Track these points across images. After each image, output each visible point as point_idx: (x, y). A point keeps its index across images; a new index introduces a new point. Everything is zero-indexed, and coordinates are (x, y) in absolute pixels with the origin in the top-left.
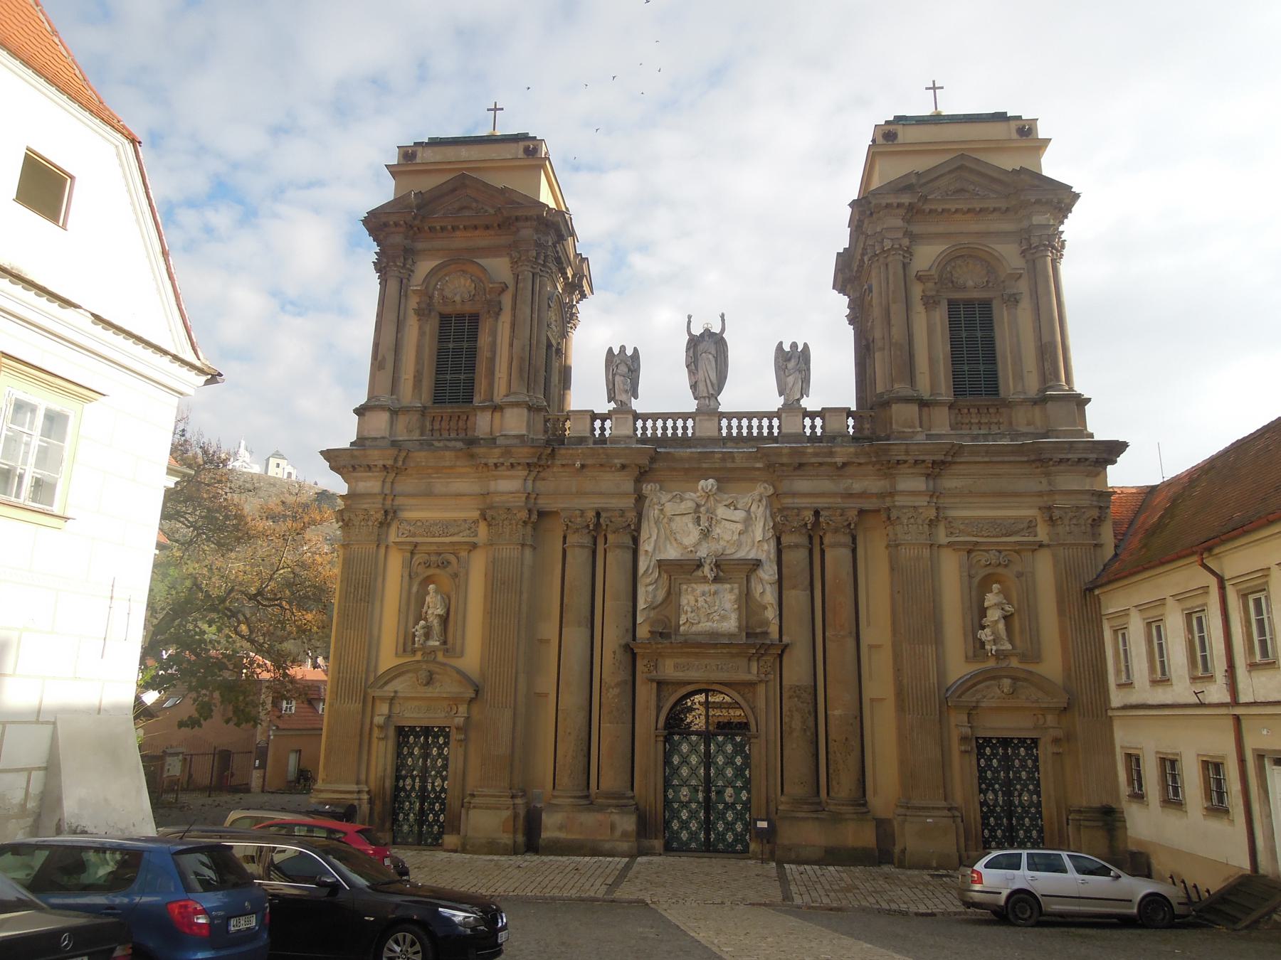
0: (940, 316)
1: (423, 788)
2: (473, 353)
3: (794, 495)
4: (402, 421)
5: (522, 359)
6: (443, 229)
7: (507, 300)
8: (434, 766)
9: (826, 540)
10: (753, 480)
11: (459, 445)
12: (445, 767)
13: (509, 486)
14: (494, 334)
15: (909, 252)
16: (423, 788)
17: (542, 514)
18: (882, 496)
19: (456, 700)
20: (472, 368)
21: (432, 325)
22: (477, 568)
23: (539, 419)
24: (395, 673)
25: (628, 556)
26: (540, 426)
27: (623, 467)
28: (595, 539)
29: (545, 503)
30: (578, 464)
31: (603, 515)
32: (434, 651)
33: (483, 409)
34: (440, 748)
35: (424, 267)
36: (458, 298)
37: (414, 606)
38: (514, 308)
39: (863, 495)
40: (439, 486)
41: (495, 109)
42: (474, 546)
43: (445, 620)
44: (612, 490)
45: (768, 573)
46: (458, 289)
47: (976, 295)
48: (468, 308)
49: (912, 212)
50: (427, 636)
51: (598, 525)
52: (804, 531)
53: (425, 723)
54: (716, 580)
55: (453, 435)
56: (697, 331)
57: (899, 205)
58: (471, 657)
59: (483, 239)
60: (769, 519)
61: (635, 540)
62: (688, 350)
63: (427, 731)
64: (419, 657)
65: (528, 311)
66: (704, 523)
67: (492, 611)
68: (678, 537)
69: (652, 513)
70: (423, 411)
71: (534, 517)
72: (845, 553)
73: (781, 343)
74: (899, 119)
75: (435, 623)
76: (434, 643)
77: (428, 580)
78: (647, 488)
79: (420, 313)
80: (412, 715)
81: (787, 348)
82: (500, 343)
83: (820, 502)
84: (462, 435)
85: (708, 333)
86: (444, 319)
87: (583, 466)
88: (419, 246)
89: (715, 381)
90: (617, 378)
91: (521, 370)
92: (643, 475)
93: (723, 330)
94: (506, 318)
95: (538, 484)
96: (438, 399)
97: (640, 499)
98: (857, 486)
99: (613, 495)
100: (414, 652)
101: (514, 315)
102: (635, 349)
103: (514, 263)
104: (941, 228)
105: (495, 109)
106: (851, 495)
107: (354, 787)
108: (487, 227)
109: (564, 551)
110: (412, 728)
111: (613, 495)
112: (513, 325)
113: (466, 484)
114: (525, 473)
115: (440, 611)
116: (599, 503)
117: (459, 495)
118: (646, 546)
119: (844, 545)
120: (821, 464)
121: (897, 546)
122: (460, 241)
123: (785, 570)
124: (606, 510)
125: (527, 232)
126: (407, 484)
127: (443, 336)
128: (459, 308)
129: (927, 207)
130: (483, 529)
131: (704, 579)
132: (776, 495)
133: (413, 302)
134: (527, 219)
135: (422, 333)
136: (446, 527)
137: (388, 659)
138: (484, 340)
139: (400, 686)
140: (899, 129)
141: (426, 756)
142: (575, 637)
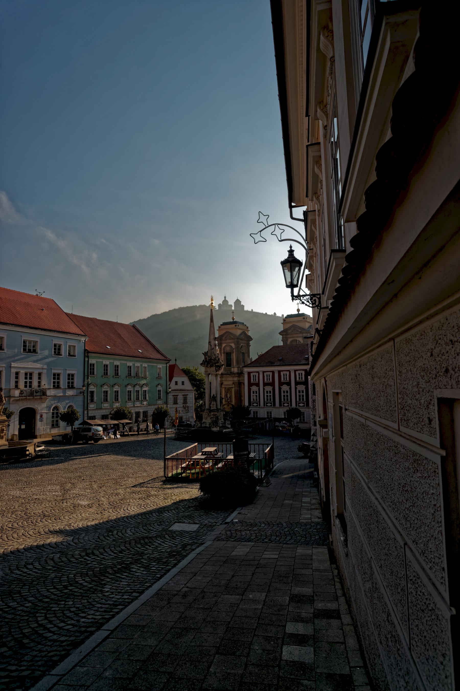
7: (234, 350)
13: (236, 379)
20: (231, 361)
21: (225, 355)
22: (233, 390)
24: (225, 405)
35: (224, 345)
40: (228, 379)
42: (232, 388)
43: (230, 397)
46: (228, 349)
58: (233, 403)
59: (230, 341)
67: (235, 397)
77: (227, 392)
79: (224, 353)
82: (234, 357)
86: (227, 353)
94: (234, 353)
103: (235, 344)
113: (231, 379)
122: (228, 341)
126: (223, 379)
133: (222, 351)
136: (229, 385)
138: (232, 357)
139: (226, 406)
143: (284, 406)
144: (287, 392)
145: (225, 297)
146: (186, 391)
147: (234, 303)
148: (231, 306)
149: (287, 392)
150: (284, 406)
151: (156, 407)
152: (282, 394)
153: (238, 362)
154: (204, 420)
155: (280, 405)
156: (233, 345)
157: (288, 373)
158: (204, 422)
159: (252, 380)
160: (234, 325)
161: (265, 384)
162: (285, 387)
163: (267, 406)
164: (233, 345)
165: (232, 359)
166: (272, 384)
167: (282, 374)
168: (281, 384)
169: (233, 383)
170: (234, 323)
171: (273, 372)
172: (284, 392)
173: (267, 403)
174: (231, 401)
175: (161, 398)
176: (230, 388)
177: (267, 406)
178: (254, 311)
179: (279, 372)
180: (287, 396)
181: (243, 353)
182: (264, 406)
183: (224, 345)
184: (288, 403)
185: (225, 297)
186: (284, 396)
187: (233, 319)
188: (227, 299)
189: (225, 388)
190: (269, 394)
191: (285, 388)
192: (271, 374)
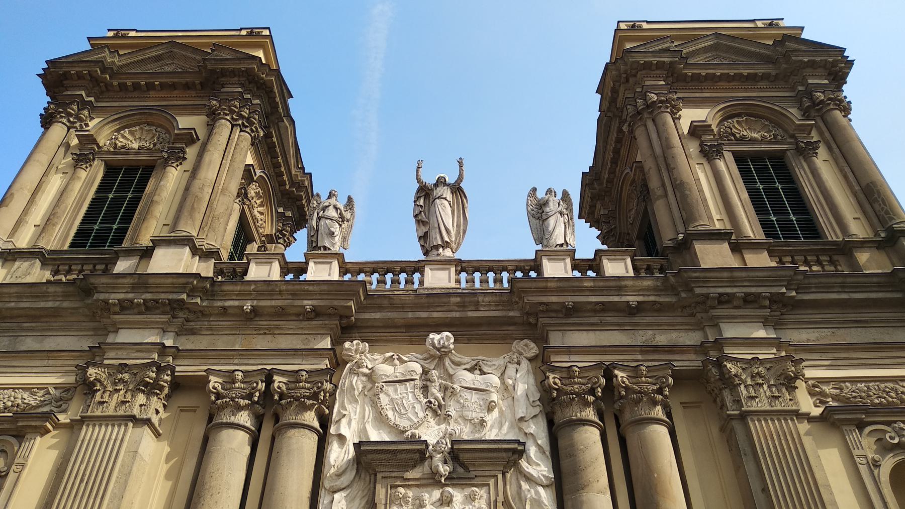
0: (727, 166)
3: (570, 350)
9: (627, 417)
10: (507, 339)
18: (701, 348)
25: (307, 443)
27: (316, 313)
28: (259, 420)
30: (248, 306)
31: (277, 378)
39: (671, 349)
45: (538, 466)
47: (764, 147)
51: (267, 393)
52: (591, 399)
54: (453, 480)
56: (429, 179)
60: (533, 389)
61: (325, 421)
62: (417, 198)
66: (435, 391)
68: (390, 414)
72: (661, 433)
73: (534, 190)
81: (541, 194)
83: (609, 358)
85: (441, 182)
87: (254, 309)
89: (450, 227)
90: (322, 222)
92: (347, 329)
93: (460, 178)
95: (183, 339)
97: (338, 363)
98: (662, 338)
102: (350, 199)
106: (656, 349)
108: (187, 86)
109: (206, 440)
114: (165, 318)
119: (658, 421)
120: (605, 308)
121: (744, 417)
123: (565, 463)
124: (283, 373)
129: (689, 72)
131: (433, 480)
132: (541, 363)
134: (234, 73)
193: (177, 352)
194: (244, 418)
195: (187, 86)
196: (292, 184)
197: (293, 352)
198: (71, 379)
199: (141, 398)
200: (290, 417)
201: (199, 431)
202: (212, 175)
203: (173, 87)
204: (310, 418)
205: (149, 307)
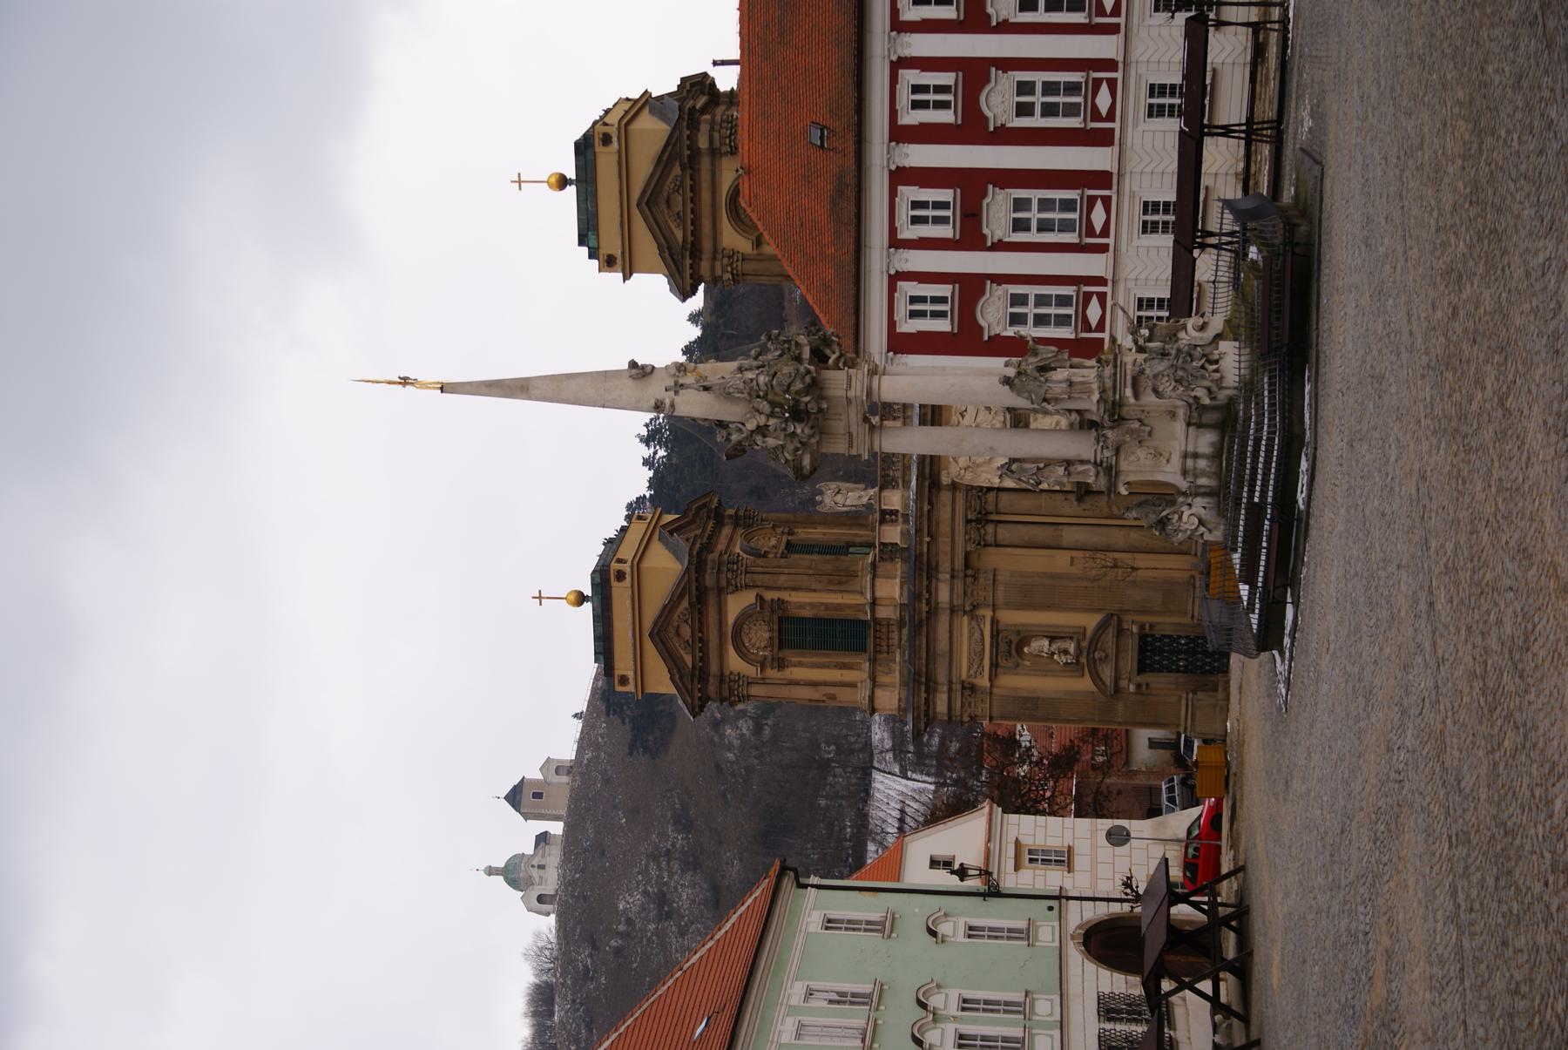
1: (1186, 652)
2: (817, 621)
4: (881, 679)
5: (830, 582)
6: (701, 650)
7: (769, 595)
8: (1170, 645)
11: (905, 631)
12: (1170, 637)
13: (943, 595)
14: (802, 606)
15: (732, 255)
16: (1186, 652)
17: (967, 566)
19: (1120, 631)
21: (792, 656)
22: (1010, 617)
23: (883, 568)
24: (1096, 678)
25: (1004, 497)
26: (889, 566)
27: (930, 503)
28: (988, 521)
29: (959, 563)
32: (1078, 647)
33: (873, 612)
34: (1156, 640)
35: (735, 663)
36: (767, 635)
37: (1043, 665)
38: (779, 589)
40: (942, 645)
41: (540, 597)
42: (994, 622)
43: (1052, 639)
44: (950, 511)
46: (759, 636)
48: (776, 627)
49: (695, 251)
50: (1066, 652)
51: (978, 521)
53: (1136, 653)
55: (895, 636)
57: (691, 266)
61: (990, 489)
63: (1142, 650)
64: (1083, 660)
65: (783, 577)
67: (1049, 607)
69: (968, 478)
70: (873, 661)
71: (970, 572)
74: (582, 241)
75: (1054, 647)
76: (1072, 648)
78: (945, 480)
79: (781, 665)
80: (1130, 661)
84: (895, 628)
87: (929, 535)
88: (714, 668)
91: (840, 583)
94: (785, 596)
96: (862, 649)
97: (954, 486)
99: (953, 509)
100: (1078, 662)
101: (786, 589)
103: (737, 589)
104: (706, 224)
105: (540, 597)
107: (1184, 702)
108: (700, 612)
110: (1140, 662)
111: (953, 509)
112: (794, 589)
115: (1046, 642)
116: (960, 521)
117: (951, 632)
118: (996, 482)
125: (709, 580)
127: (801, 646)
128: (776, 634)
129: (690, 239)
130: (981, 612)
133: (772, 673)
134: (697, 580)
135: (801, 664)
137: (1085, 684)
138: (807, 613)
139: (1107, 673)
140: (604, 251)
141: (1161, 651)
142: (1071, 536)
143: (1111, 116)
144: (1025, 88)
145: (491, 871)
146: (995, 847)
147: (526, 817)
148: (542, 839)
149: (1025, 88)
150: (1111, 116)
151: (1075, 955)
152: (1036, 121)
153: (842, 579)
154: (1170, 473)
155: (1103, 139)
156: (736, 604)
157: (911, 76)
158: (1185, 473)
159: (943, 326)
160: (614, 583)
161: (971, 237)
162: (996, 99)
163: (1105, 232)
164: (736, 604)
165: (822, 613)
166: (973, 184)
167: (911, 118)
168: (973, 129)
169: (972, 613)
170: (603, 577)
171: (901, 176)
172: (1024, 110)
173: (1090, 232)
174: (1077, 634)
175: (1021, 924)
176: (995, 634)
177: (1105, 232)
178: (582, 706)
179: (901, 135)
180: (1050, 88)
181: (790, 547)
182: (1103, 249)
183: (735, 663)
184: (1097, 84)
185: (491, 871)
186: (1049, 110)
187: (580, 599)
188: (500, 863)
189: (994, 666)
190: (1034, 215)
191: (999, 102)
192: (910, 193)
193: (953, 570)
194: (990, 528)
195: (700, 612)
196: (709, 517)
197: (950, 511)
198: (966, 619)
199: (982, 580)
200: (990, 508)
201: (993, 550)
202: (805, 578)
203: (700, 622)
204: (991, 496)
205: (929, 591)
